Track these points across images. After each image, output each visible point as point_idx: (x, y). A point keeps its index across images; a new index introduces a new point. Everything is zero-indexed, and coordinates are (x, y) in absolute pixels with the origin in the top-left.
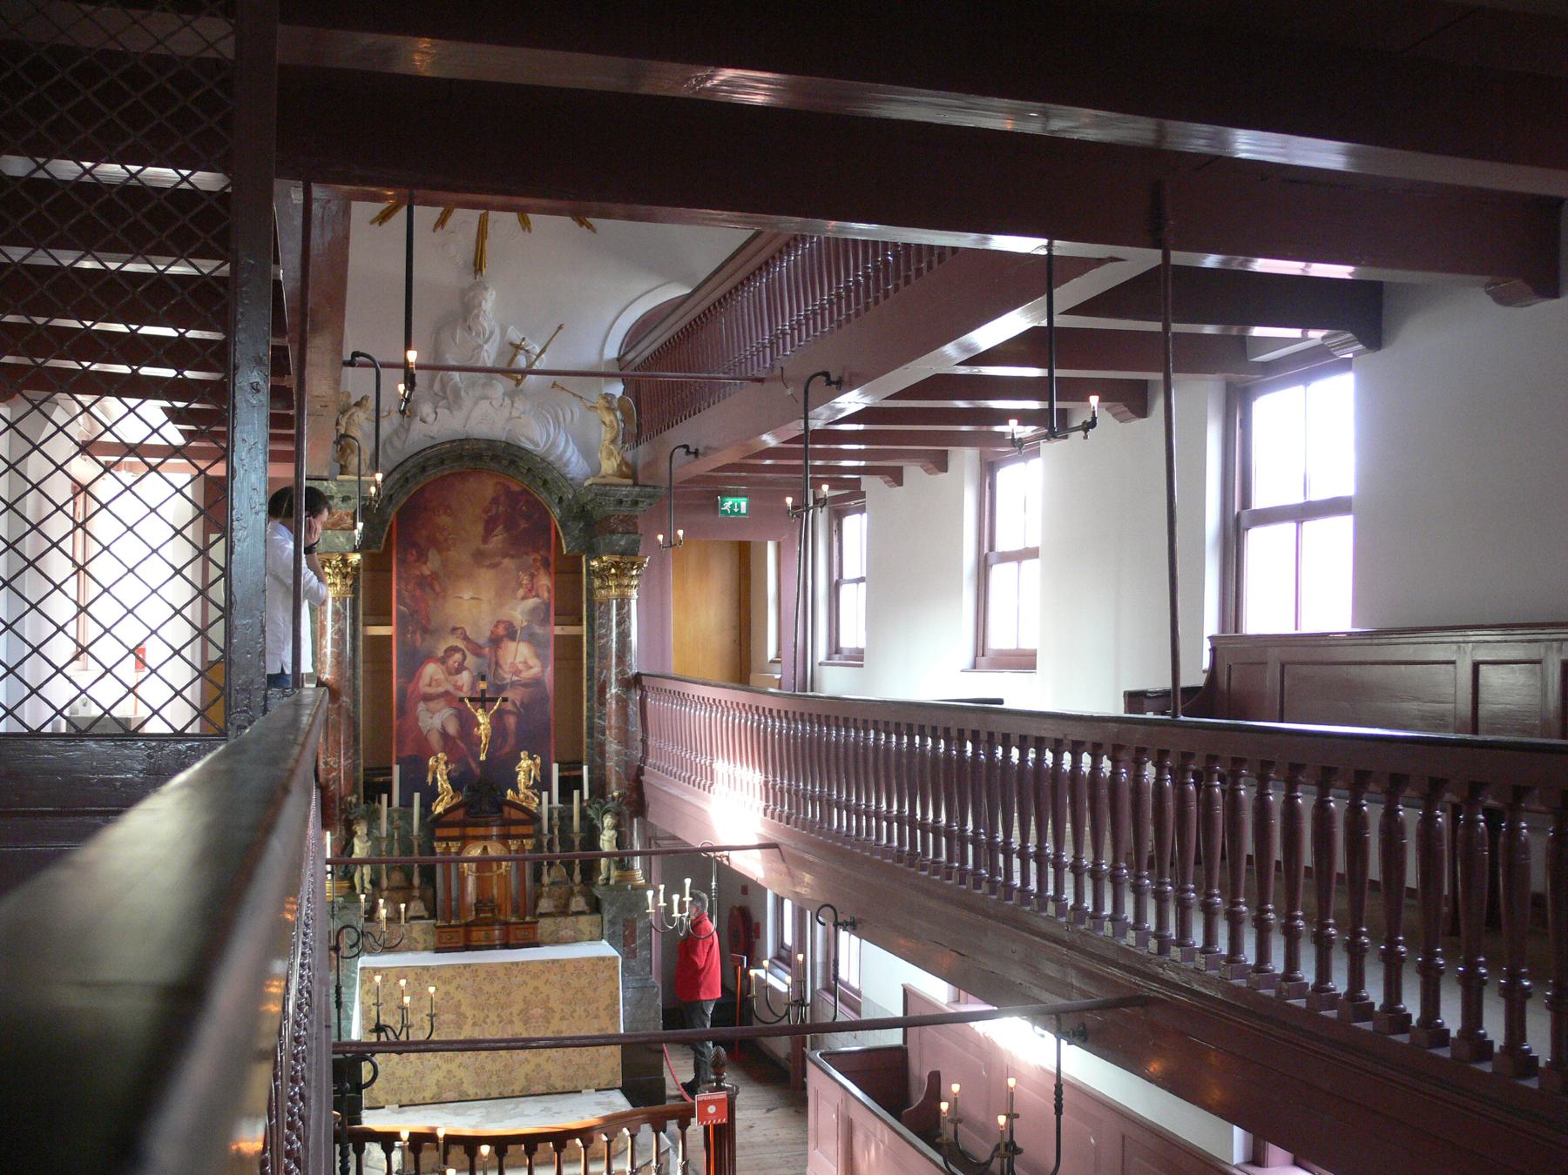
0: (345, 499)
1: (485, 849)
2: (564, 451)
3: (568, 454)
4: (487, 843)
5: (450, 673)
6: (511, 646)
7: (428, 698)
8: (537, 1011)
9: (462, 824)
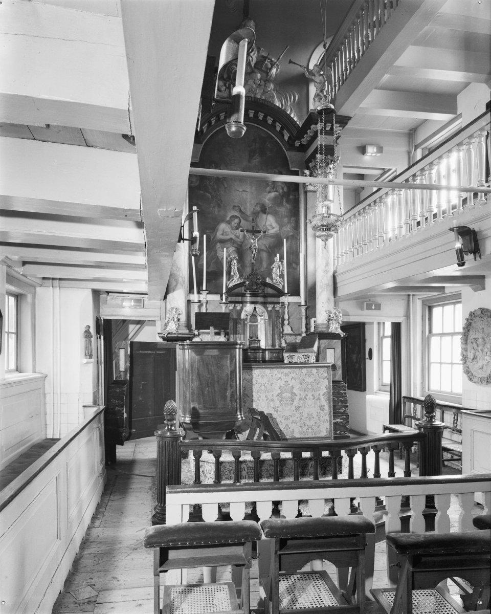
1: (255, 309)
5: (233, 230)
6: (264, 216)
7: (223, 242)
8: (287, 395)
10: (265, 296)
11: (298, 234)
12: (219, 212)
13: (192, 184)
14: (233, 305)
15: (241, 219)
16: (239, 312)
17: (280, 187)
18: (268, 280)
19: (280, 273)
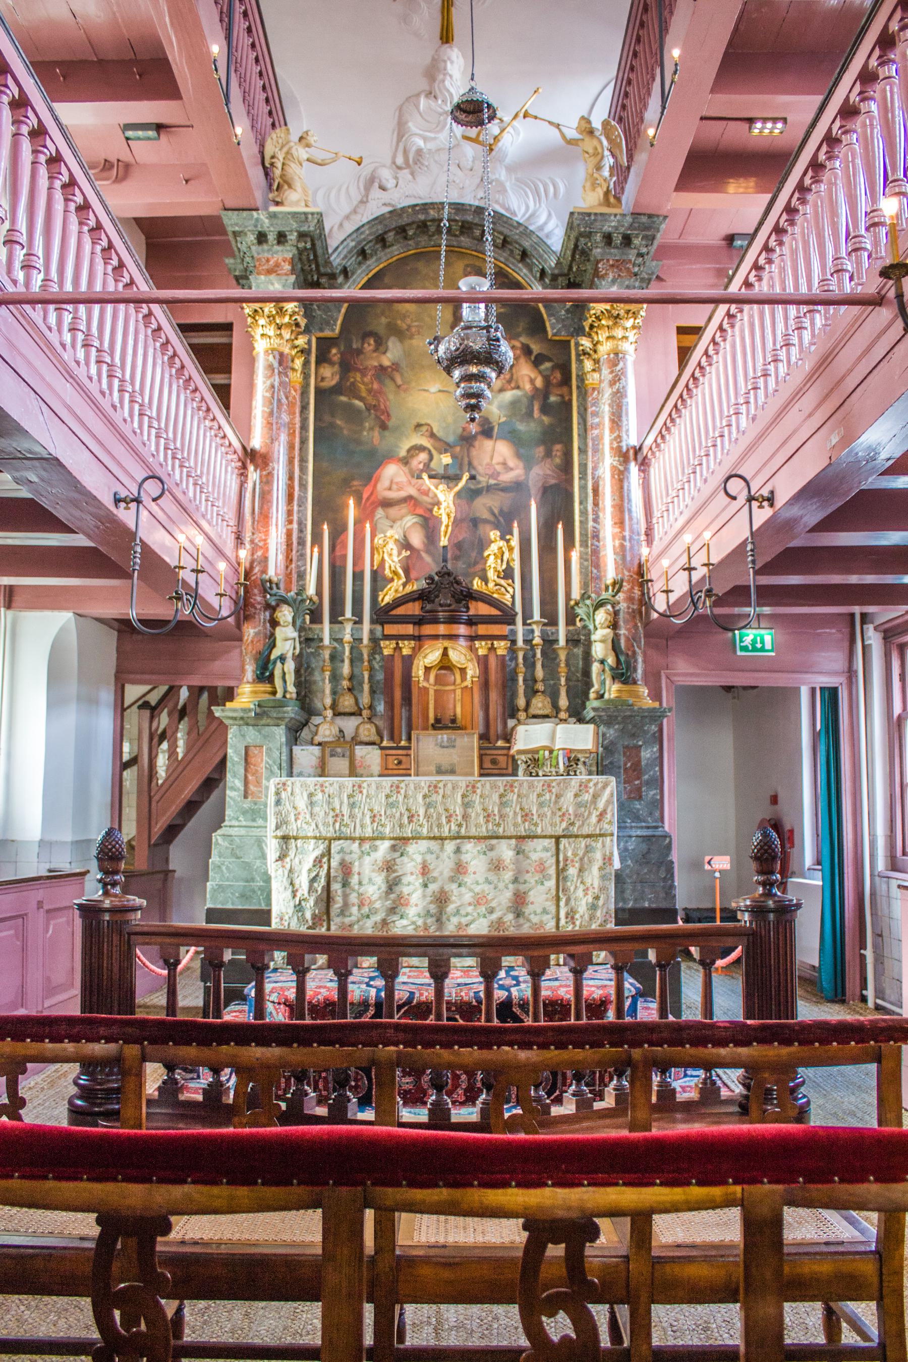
0: (281, 238)
2: (546, 223)
3: (548, 229)
4: (446, 643)
6: (488, 444)
7: (387, 504)
9: (419, 622)
10: (471, 622)
11: (570, 481)
12: (382, 437)
13: (326, 384)
14: (393, 644)
15: (434, 452)
16: (408, 662)
17: (526, 379)
18: (477, 584)
19: (504, 567)
